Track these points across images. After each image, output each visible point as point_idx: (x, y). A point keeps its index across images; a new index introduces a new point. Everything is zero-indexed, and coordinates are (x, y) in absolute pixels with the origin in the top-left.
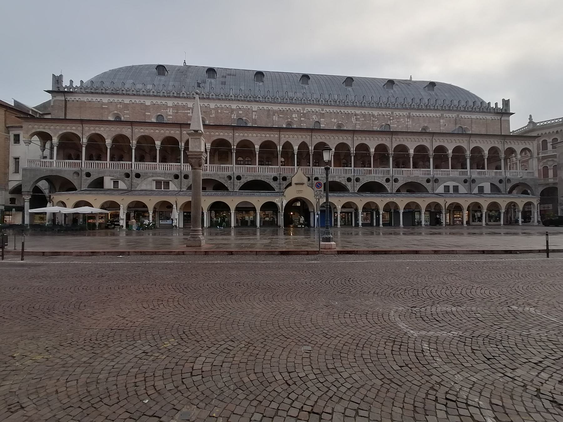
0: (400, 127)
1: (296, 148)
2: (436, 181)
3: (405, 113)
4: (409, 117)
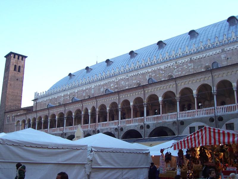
0: (184, 73)
2: (182, 123)
3: (187, 59)
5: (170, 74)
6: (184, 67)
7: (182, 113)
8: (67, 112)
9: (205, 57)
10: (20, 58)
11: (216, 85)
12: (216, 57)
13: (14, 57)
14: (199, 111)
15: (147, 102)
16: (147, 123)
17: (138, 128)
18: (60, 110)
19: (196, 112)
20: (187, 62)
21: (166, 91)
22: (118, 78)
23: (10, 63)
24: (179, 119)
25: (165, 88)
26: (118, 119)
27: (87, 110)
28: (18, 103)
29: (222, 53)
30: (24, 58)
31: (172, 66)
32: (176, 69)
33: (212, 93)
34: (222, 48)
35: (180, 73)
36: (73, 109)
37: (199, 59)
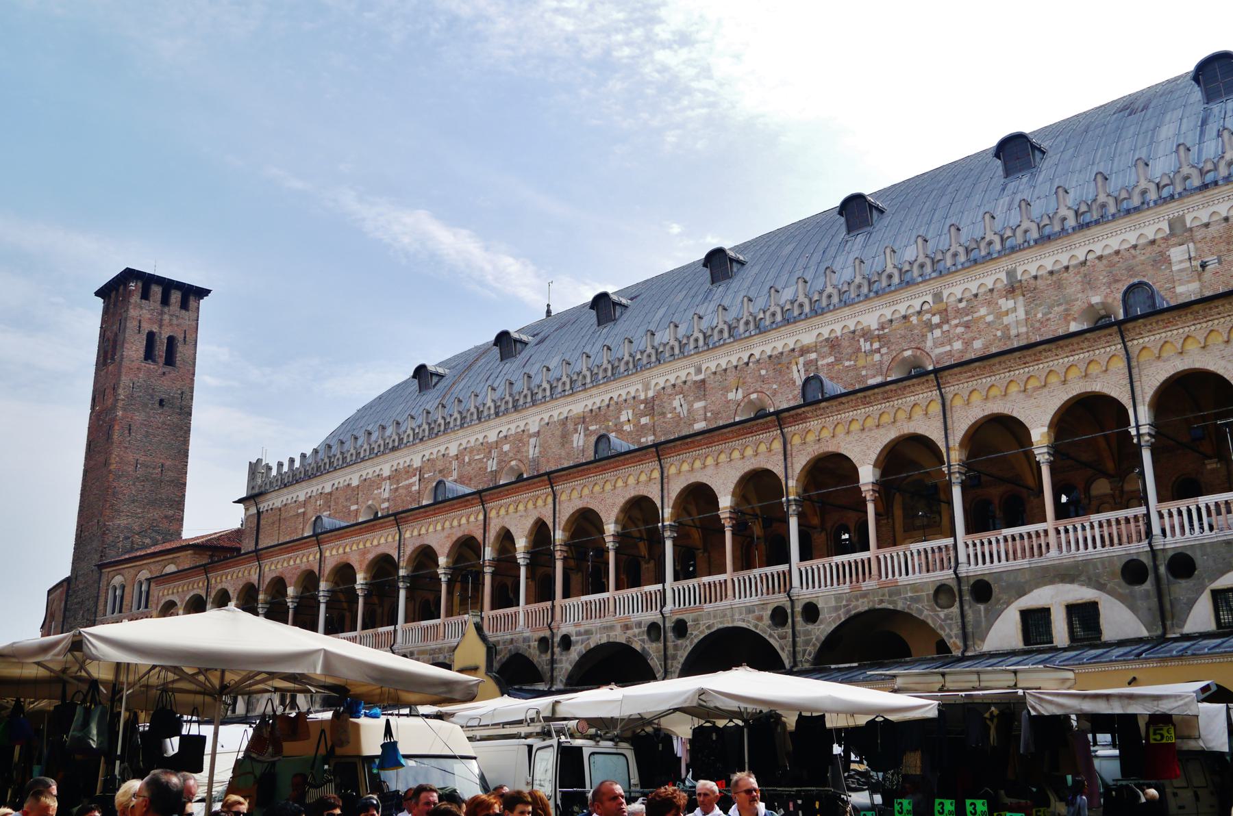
0: (978, 344)
1: (521, 543)
2: (982, 590)
3: (992, 277)
4: (1013, 288)
5: (908, 353)
6: (975, 315)
7: (1070, 528)
8: (409, 550)
9: (1084, 263)
10: (176, 296)
11: (1148, 399)
12: (1143, 258)
13: (145, 295)
14: (1067, 531)
15: (800, 490)
16: (803, 594)
17: (760, 618)
18: (375, 543)
19: (1052, 533)
20: (991, 290)
21: (892, 434)
22: (653, 383)
23: (122, 323)
24: (963, 570)
25: (886, 419)
26: (661, 579)
27: (506, 538)
28: (166, 517)
29: (1173, 240)
30: (192, 298)
31: (919, 313)
32: (939, 326)
33: (1131, 438)
34: (1173, 210)
35: (958, 345)
36: (439, 535)
37: (1051, 273)
